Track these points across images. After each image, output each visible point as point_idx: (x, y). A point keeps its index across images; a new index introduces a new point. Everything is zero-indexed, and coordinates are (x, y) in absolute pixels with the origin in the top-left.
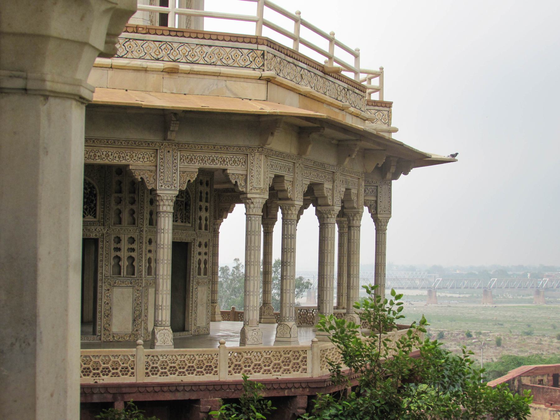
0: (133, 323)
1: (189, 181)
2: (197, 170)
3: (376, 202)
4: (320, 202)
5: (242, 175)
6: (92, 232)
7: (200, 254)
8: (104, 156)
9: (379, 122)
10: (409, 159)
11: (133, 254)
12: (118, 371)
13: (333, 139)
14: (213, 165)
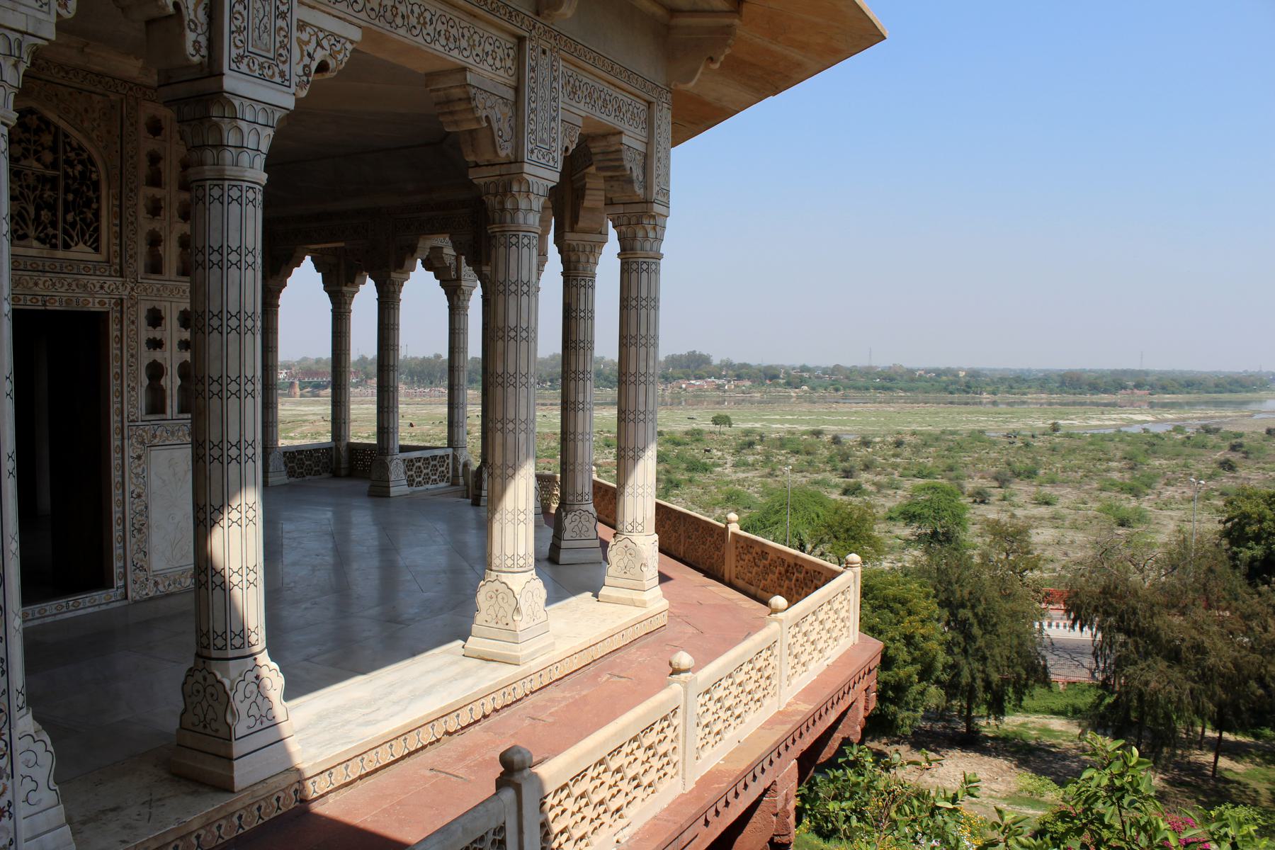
6: (92, 294)
8: (413, 21)
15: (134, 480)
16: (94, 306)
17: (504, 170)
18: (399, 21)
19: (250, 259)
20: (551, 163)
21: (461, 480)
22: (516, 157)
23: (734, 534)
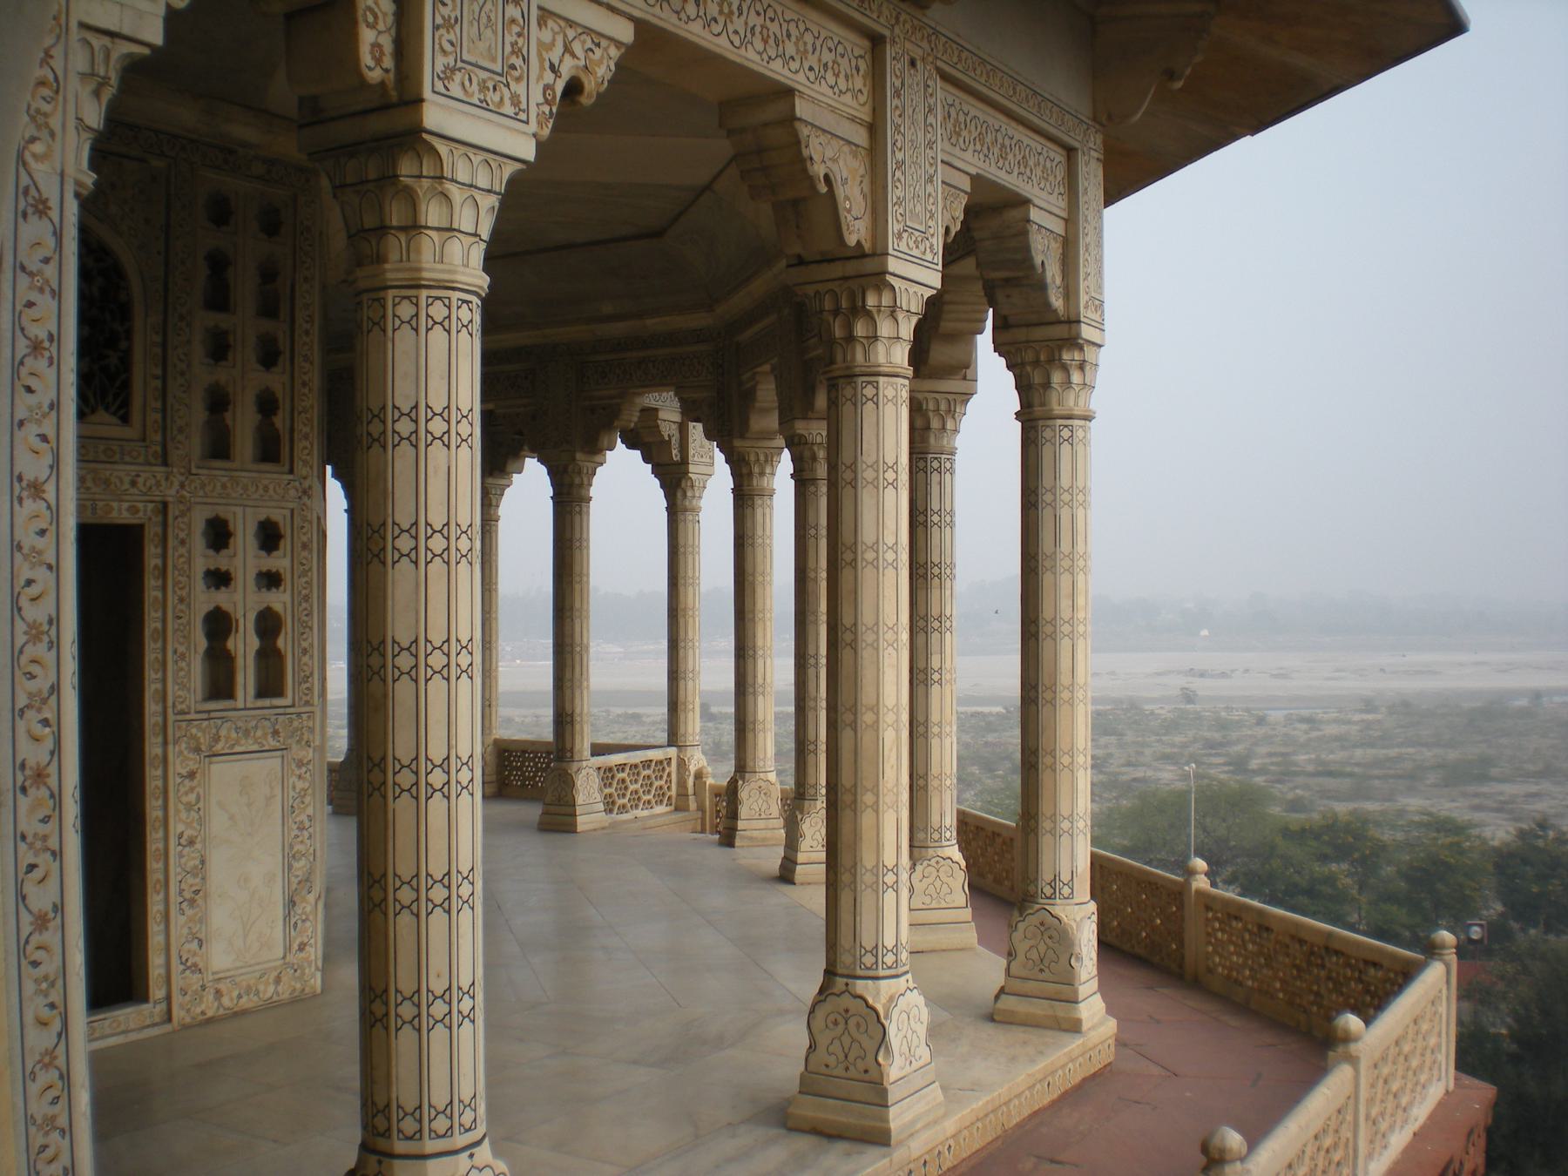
0: (287, 916)
14: (1002, 174)
15: (183, 815)
17: (851, 268)
19: (464, 429)
20: (929, 257)
21: (693, 805)
22: (874, 245)
23: (1199, 893)
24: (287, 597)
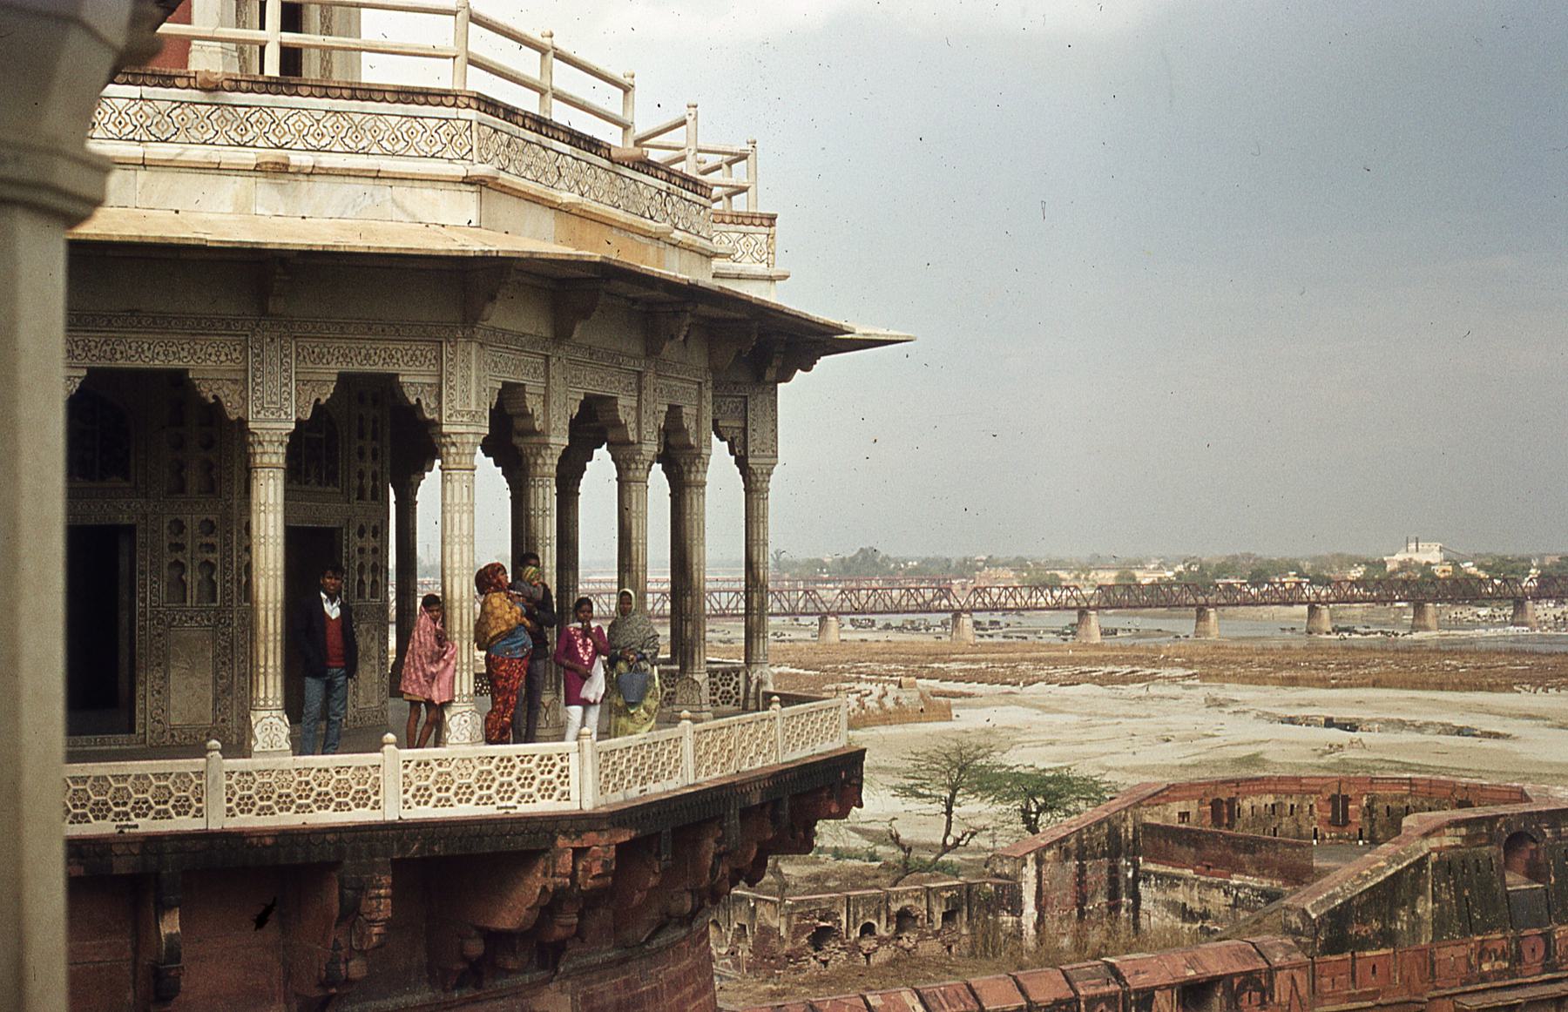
0: (215, 705)
1: (318, 400)
2: (335, 378)
3: (745, 430)
4: (611, 436)
5: (430, 385)
7: (361, 550)
9: (748, 259)
10: (801, 342)
11: (212, 557)
12: (169, 806)
13: (635, 301)
16: (124, 519)
18: (118, 356)
24: (218, 555)
